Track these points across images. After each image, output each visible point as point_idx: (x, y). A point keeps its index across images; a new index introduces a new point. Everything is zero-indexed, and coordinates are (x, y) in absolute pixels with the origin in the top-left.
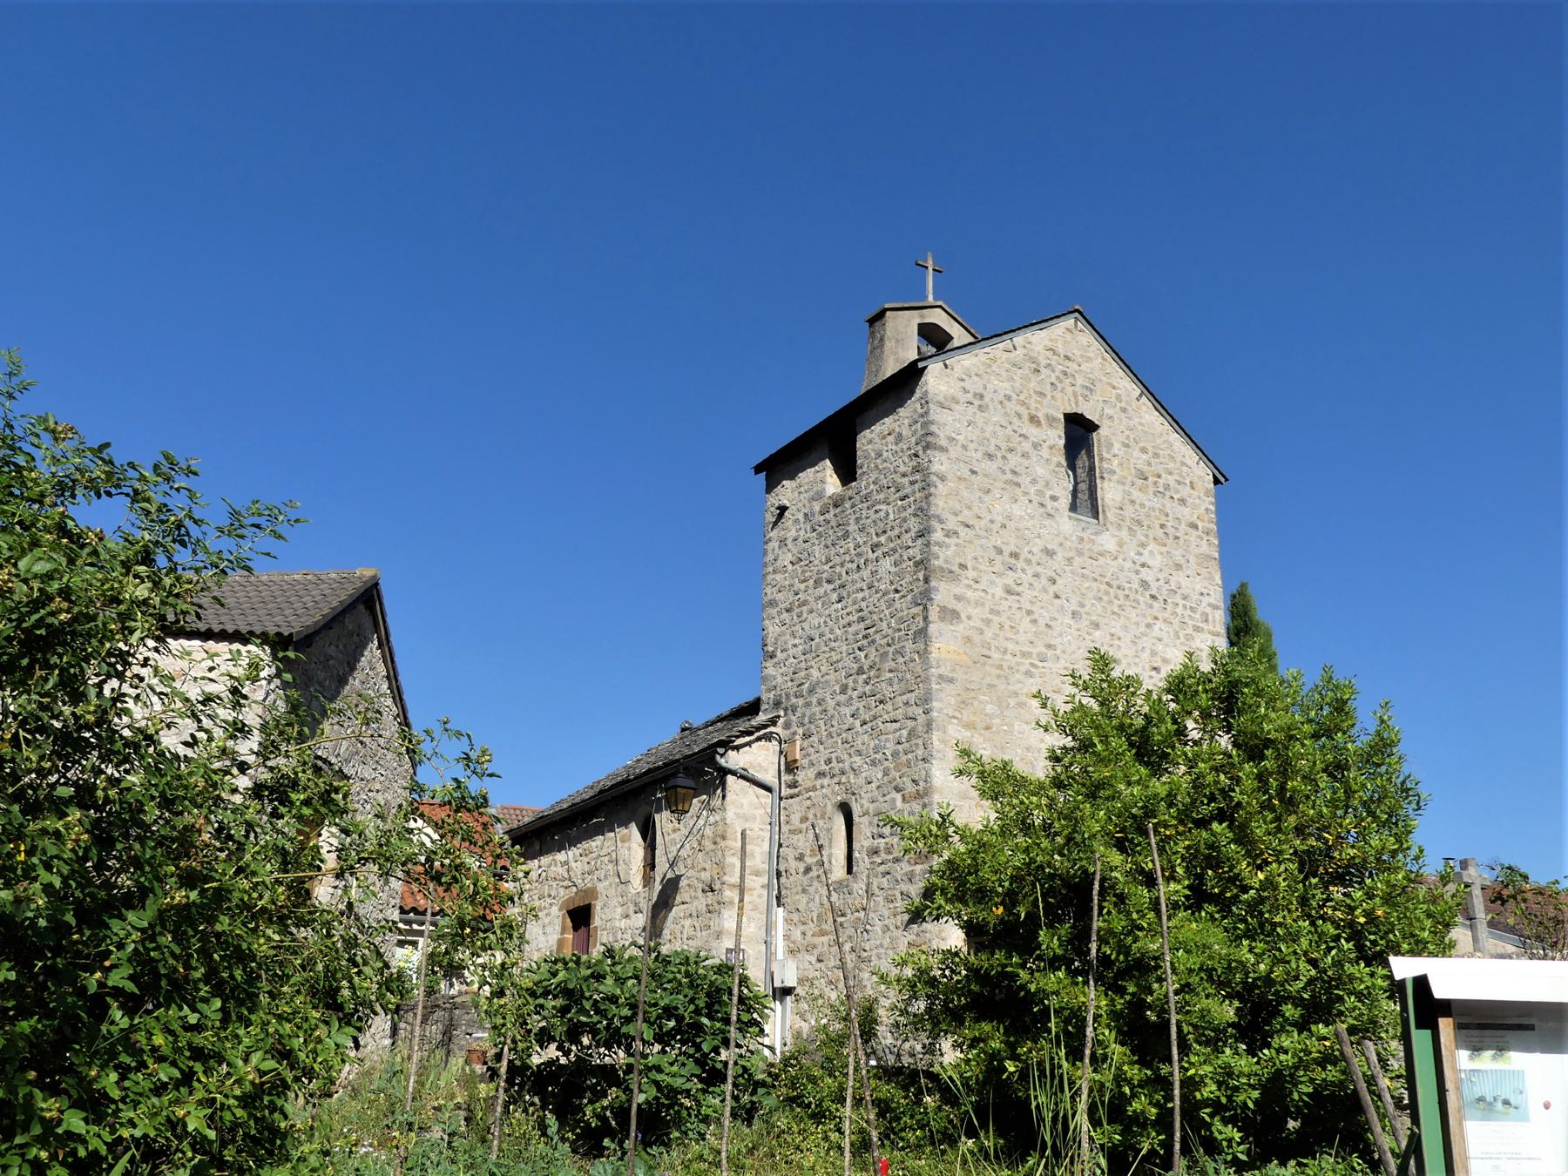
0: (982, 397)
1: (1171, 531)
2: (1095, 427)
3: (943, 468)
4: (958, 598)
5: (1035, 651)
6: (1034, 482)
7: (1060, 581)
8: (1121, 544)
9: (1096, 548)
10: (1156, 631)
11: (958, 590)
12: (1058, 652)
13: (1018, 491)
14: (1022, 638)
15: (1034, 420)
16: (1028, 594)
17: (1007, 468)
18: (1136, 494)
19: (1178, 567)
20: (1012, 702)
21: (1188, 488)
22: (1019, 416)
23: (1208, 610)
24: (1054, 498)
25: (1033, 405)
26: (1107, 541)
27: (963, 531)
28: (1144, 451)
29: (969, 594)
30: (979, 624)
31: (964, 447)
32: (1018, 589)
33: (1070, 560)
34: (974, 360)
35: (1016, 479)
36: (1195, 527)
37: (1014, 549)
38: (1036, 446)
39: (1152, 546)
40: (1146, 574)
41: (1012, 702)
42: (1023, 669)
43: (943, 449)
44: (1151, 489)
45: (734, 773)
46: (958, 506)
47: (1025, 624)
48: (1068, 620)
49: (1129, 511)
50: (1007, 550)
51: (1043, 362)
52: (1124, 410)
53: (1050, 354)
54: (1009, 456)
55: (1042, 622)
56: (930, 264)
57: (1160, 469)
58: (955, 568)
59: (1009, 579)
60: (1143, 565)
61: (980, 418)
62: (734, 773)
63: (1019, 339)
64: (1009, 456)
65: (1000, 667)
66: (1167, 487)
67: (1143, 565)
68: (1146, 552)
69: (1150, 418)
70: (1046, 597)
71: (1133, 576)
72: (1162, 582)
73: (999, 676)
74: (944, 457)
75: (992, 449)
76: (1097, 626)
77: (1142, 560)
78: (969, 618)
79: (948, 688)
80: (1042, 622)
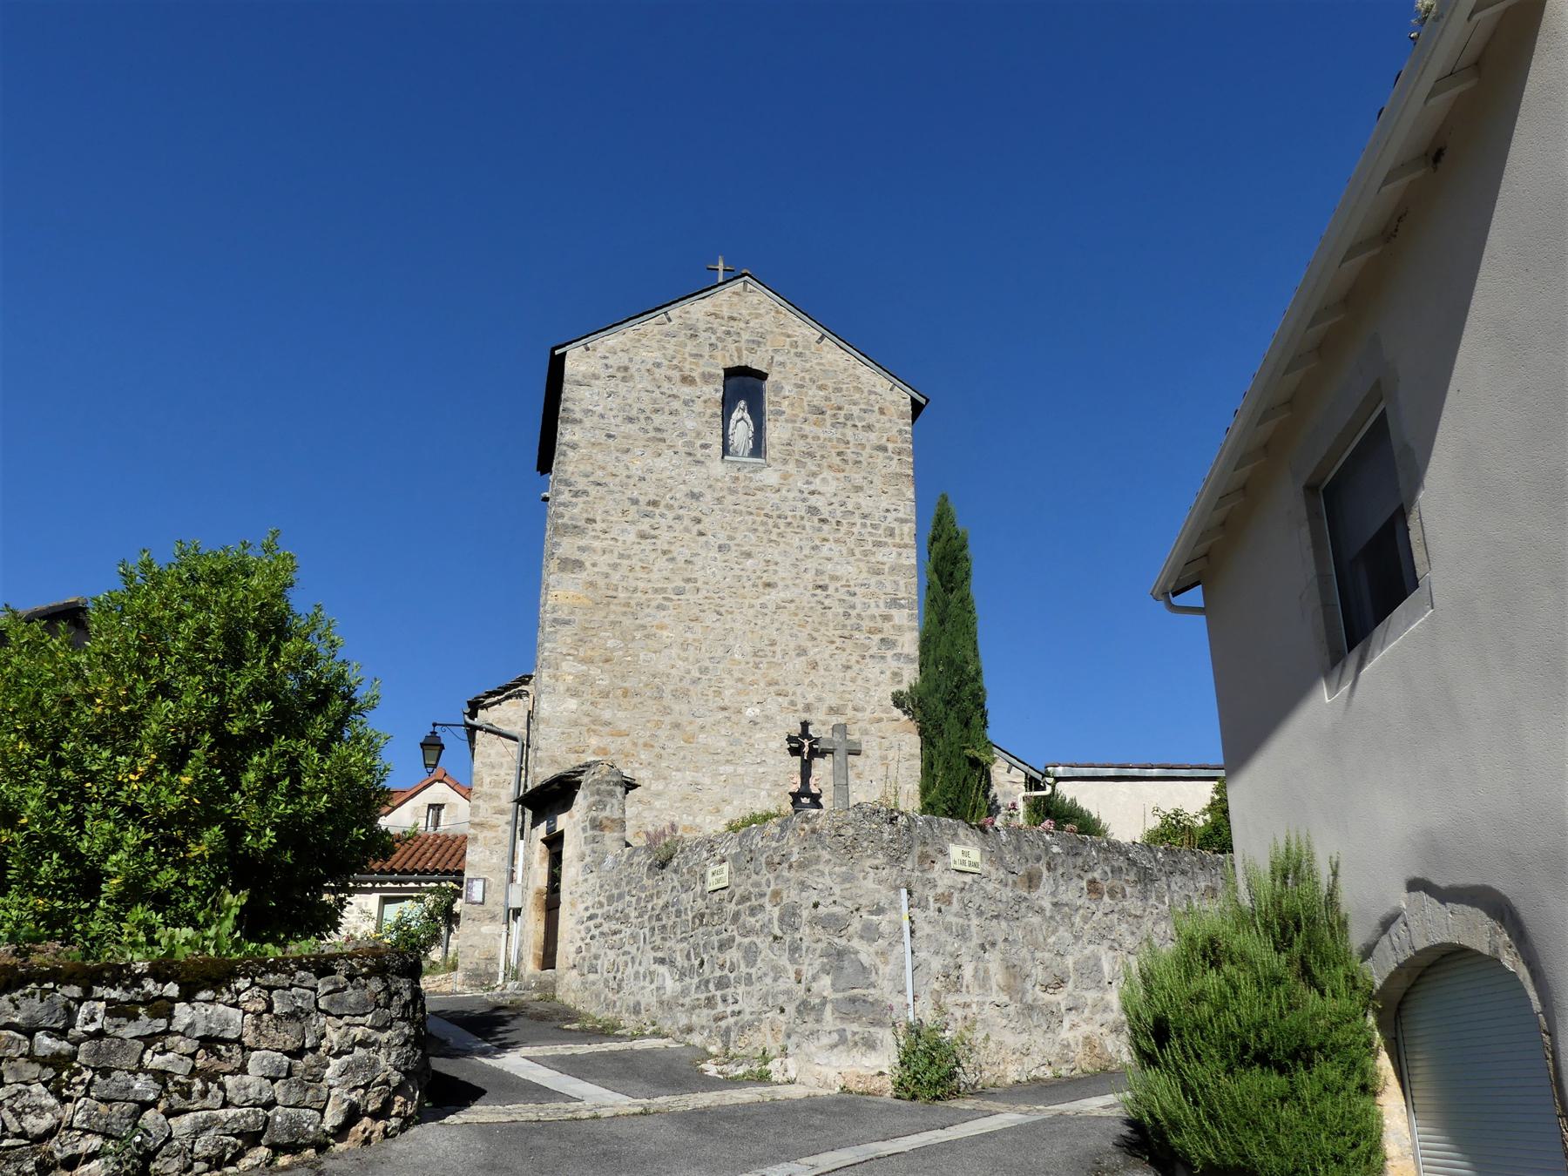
0: (626, 369)
1: (850, 457)
2: (763, 376)
3: (575, 438)
4: (582, 549)
5: (670, 586)
6: (682, 434)
7: (705, 520)
8: (785, 476)
9: (753, 485)
10: (825, 551)
11: (582, 543)
12: (699, 584)
13: (662, 446)
14: (655, 576)
15: (687, 380)
16: (665, 536)
17: (650, 428)
18: (807, 428)
19: (858, 489)
20: (638, 635)
21: (877, 415)
22: (669, 379)
23: (895, 525)
24: (704, 446)
25: (687, 366)
26: (770, 477)
27: (593, 490)
28: (821, 388)
29: (596, 544)
30: (605, 569)
31: (602, 416)
32: (653, 532)
33: (719, 500)
34: (621, 338)
35: (659, 435)
36: (885, 449)
37: (652, 497)
38: (686, 403)
39: (827, 474)
40: (814, 501)
41: (638, 635)
42: (654, 604)
43: (575, 421)
44: (829, 422)
45: (480, 728)
46: (589, 469)
47: (661, 562)
48: (714, 553)
49: (800, 446)
50: (643, 500)
51: (702, 326)
52: (799, 355)
53: (711, 319)
54: (653, 416)
55: (680, 559)
56: (721, 266)
57: (841, 401)
58: (582, 523)
59: (645, 525)
60: (813, 493)
61: (622, 389)
62: (480, 728)
63: (674, 312)
64: (653, 416)
65: (628, 605)
66: (849, 417)
67: (813, 493)
68: (818, 481)
69: (835, 356)
70: (687, 536)
71: (799, 504)
72: (836, 506)
73: (625, 614)
74: (577, 428)
75: (634, 413)
76: (749, 555)
77: (812, 488)
78: (594, 565)
79: (566, 630)
80: (680, 559)
